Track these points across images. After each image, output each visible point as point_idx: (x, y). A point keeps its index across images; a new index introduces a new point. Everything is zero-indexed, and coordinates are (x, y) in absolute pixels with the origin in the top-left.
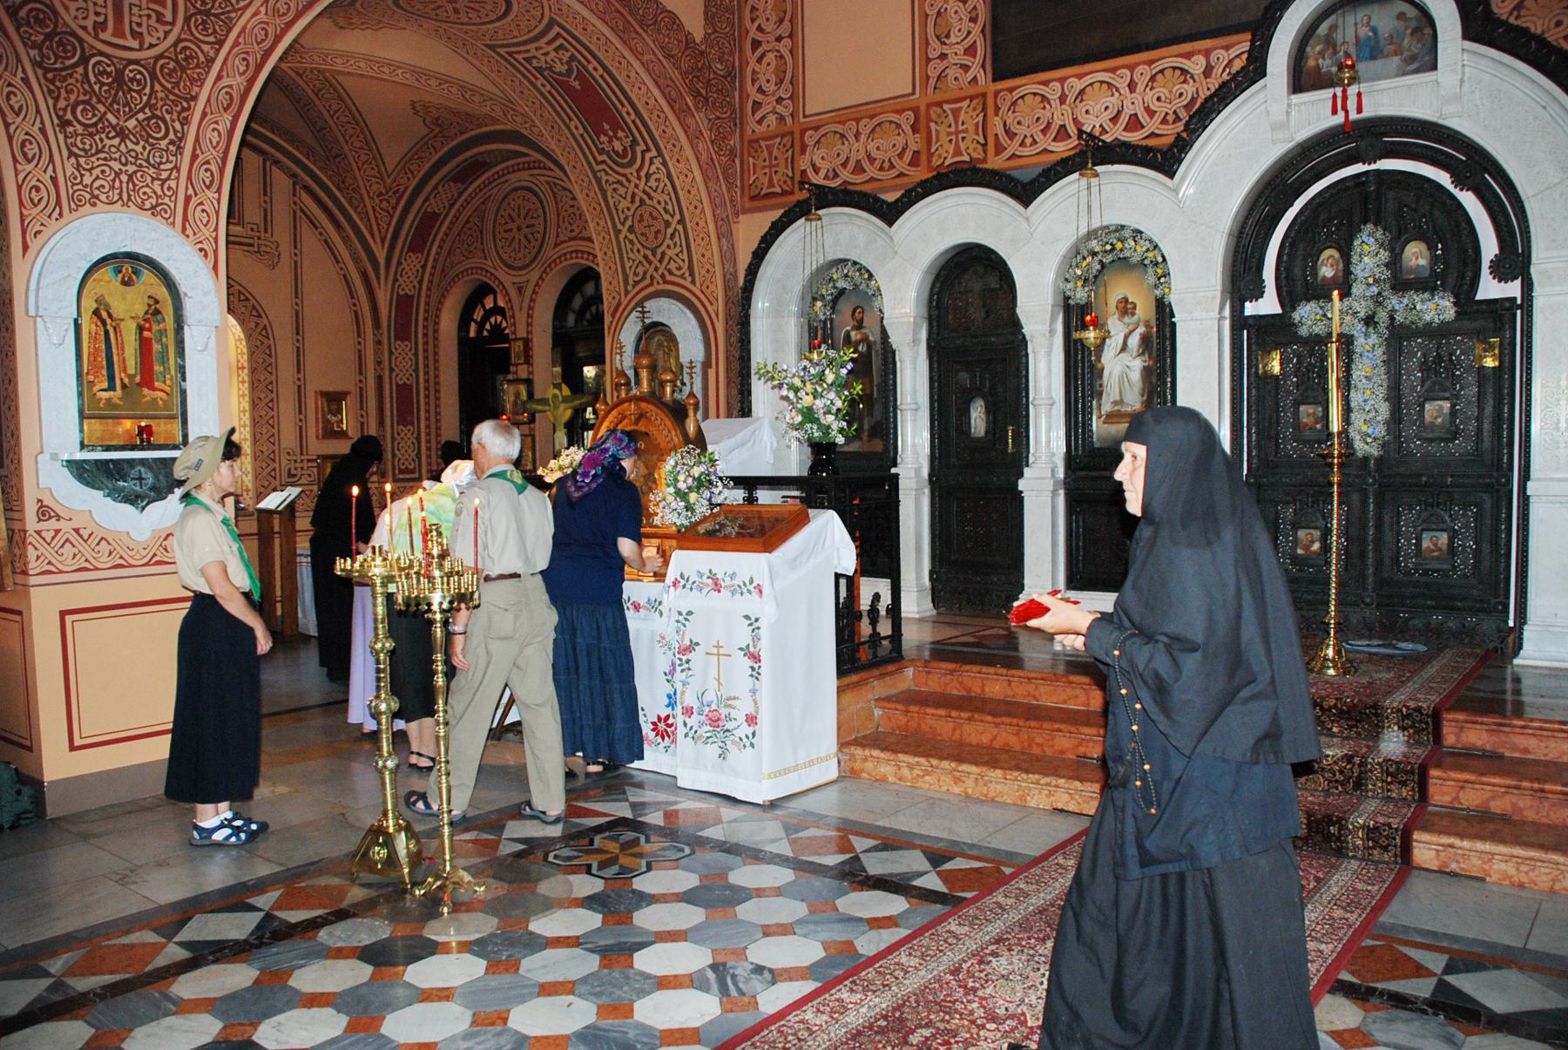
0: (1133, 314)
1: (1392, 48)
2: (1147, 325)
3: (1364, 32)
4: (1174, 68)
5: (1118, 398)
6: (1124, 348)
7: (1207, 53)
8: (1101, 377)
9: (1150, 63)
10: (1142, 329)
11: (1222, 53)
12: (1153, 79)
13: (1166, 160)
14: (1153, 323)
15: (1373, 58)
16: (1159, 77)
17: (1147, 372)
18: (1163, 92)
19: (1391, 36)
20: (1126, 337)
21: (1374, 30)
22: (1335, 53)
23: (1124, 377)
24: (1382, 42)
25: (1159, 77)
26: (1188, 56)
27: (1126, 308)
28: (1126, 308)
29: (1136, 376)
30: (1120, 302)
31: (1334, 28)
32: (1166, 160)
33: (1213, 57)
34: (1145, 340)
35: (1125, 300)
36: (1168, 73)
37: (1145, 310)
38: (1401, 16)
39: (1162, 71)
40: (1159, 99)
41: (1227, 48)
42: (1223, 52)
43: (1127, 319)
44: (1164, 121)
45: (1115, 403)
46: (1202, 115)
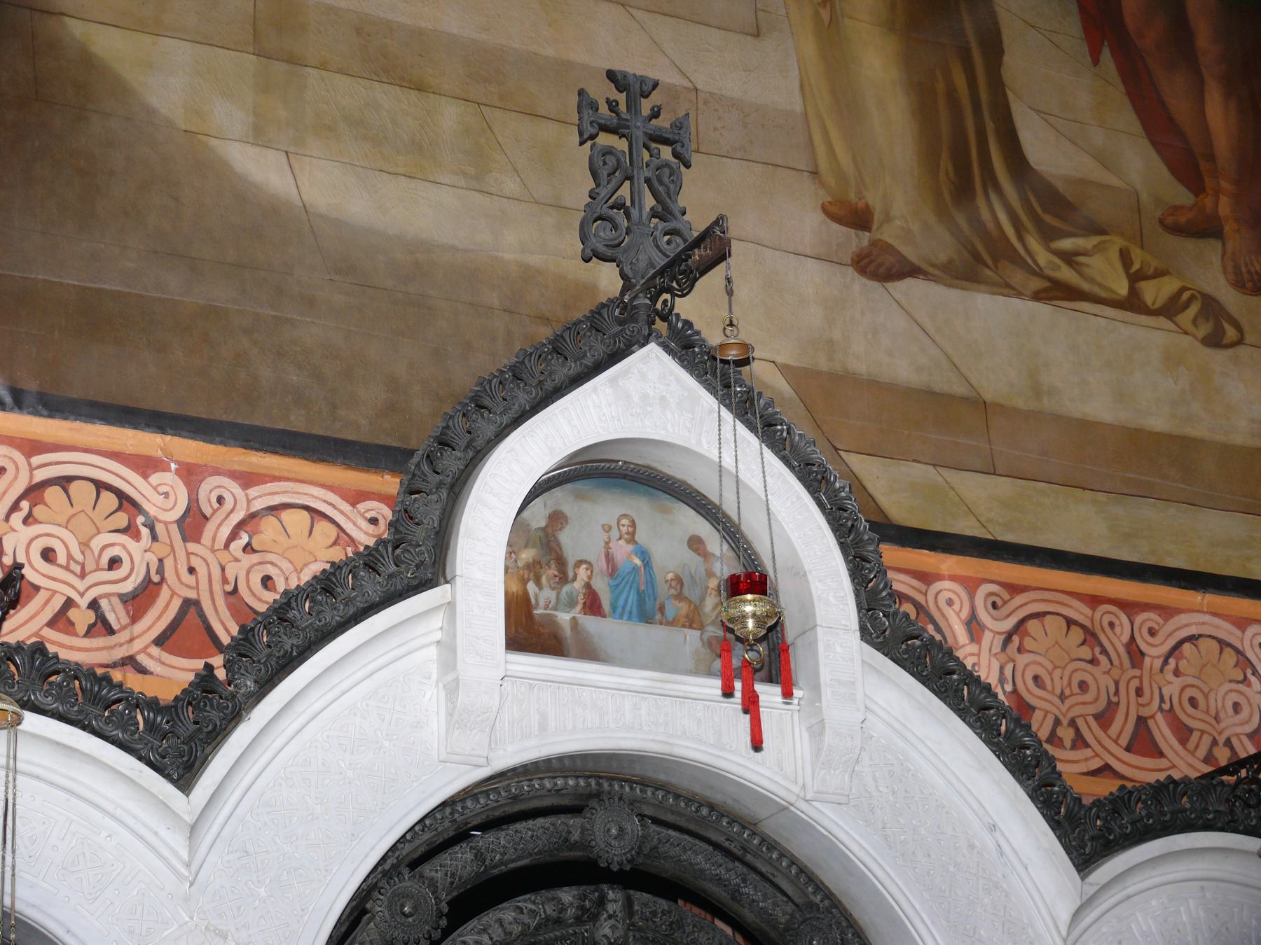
1: (683, 608)
3: (622, 550)
4: (100, 486)
7: (191, 474)
9: (32, 447)
11: (232, 489)
12: (34, 492)
13: (179, 738)
15: (645, 617)
16: (53, 493)
18: (65, 542)
19: (679, 580)
21: (644, 555)
22: (563, 578)
24: (663, 590)
25: (53, 493)
26: (145, 465)
32: (179, 738)
33: (209, 488)
36: (83, 491)
38: (696, 544)
39: (64, 482)
40: (48, 555)
41: (248, 480)
42: (235, 487)
44: (60, 620)
46: (281, 638)
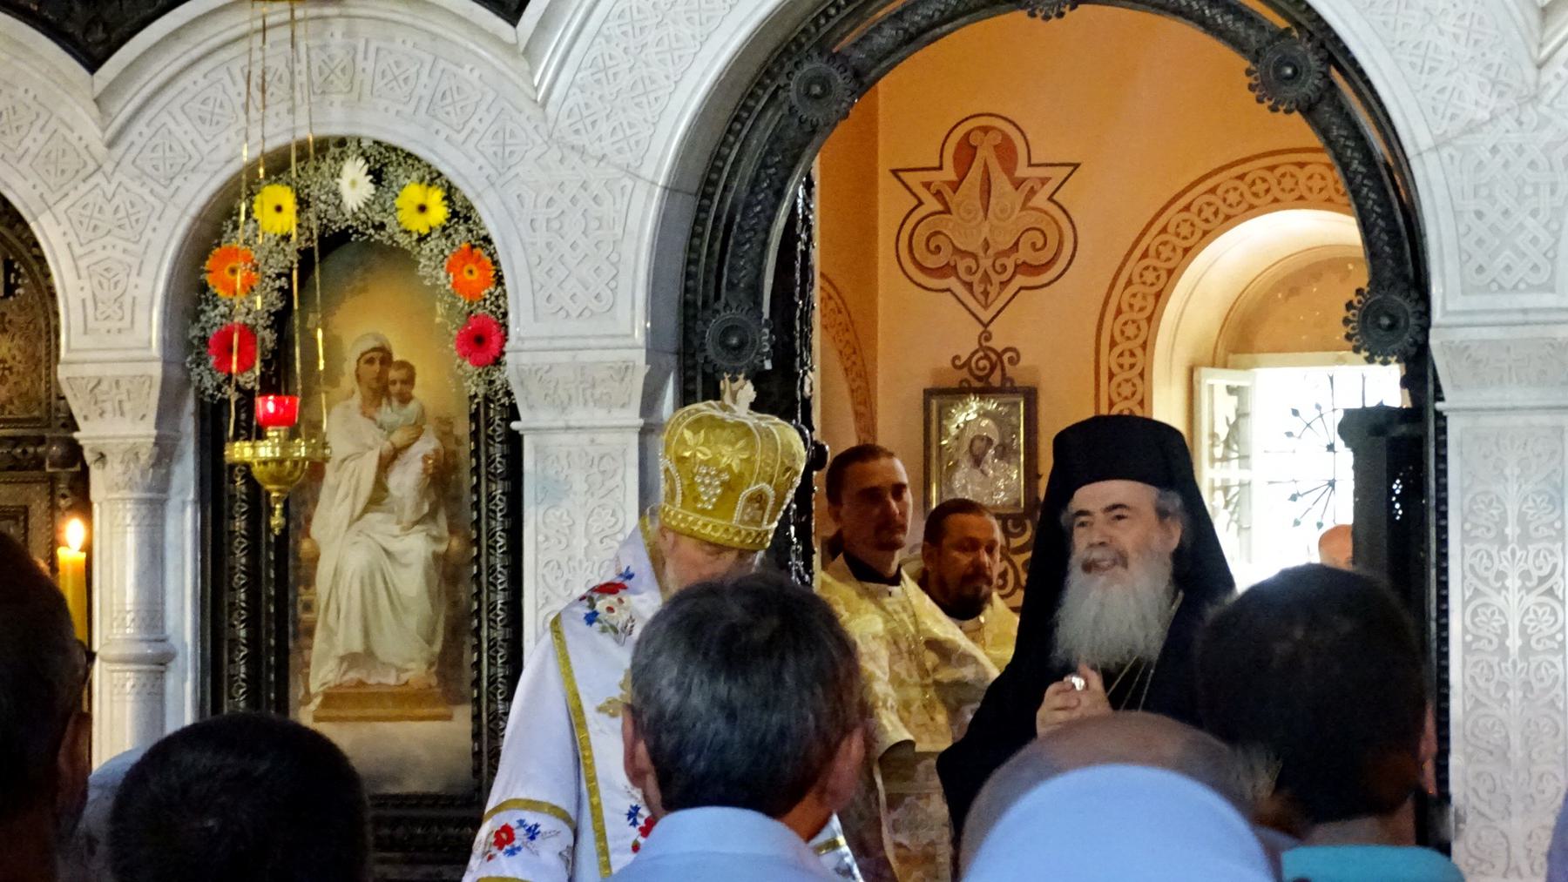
0: (405, 399)
2: (445, 434)
5: (357, 646)
6: (379, 497)
8: (309, 582)
10: (427, 445)
14: (463, 428)
17: (446, 572)
20: (386, 463)
23: (376, 581)
27: (385, 379)
28: (385, 379)
29: (412, 581)
30: (367, 359)
31: (483, 268)
34: (440, 479)
35: (383, 356)
37: (442, 380)
43: (388, 413)
45: (351, 660)
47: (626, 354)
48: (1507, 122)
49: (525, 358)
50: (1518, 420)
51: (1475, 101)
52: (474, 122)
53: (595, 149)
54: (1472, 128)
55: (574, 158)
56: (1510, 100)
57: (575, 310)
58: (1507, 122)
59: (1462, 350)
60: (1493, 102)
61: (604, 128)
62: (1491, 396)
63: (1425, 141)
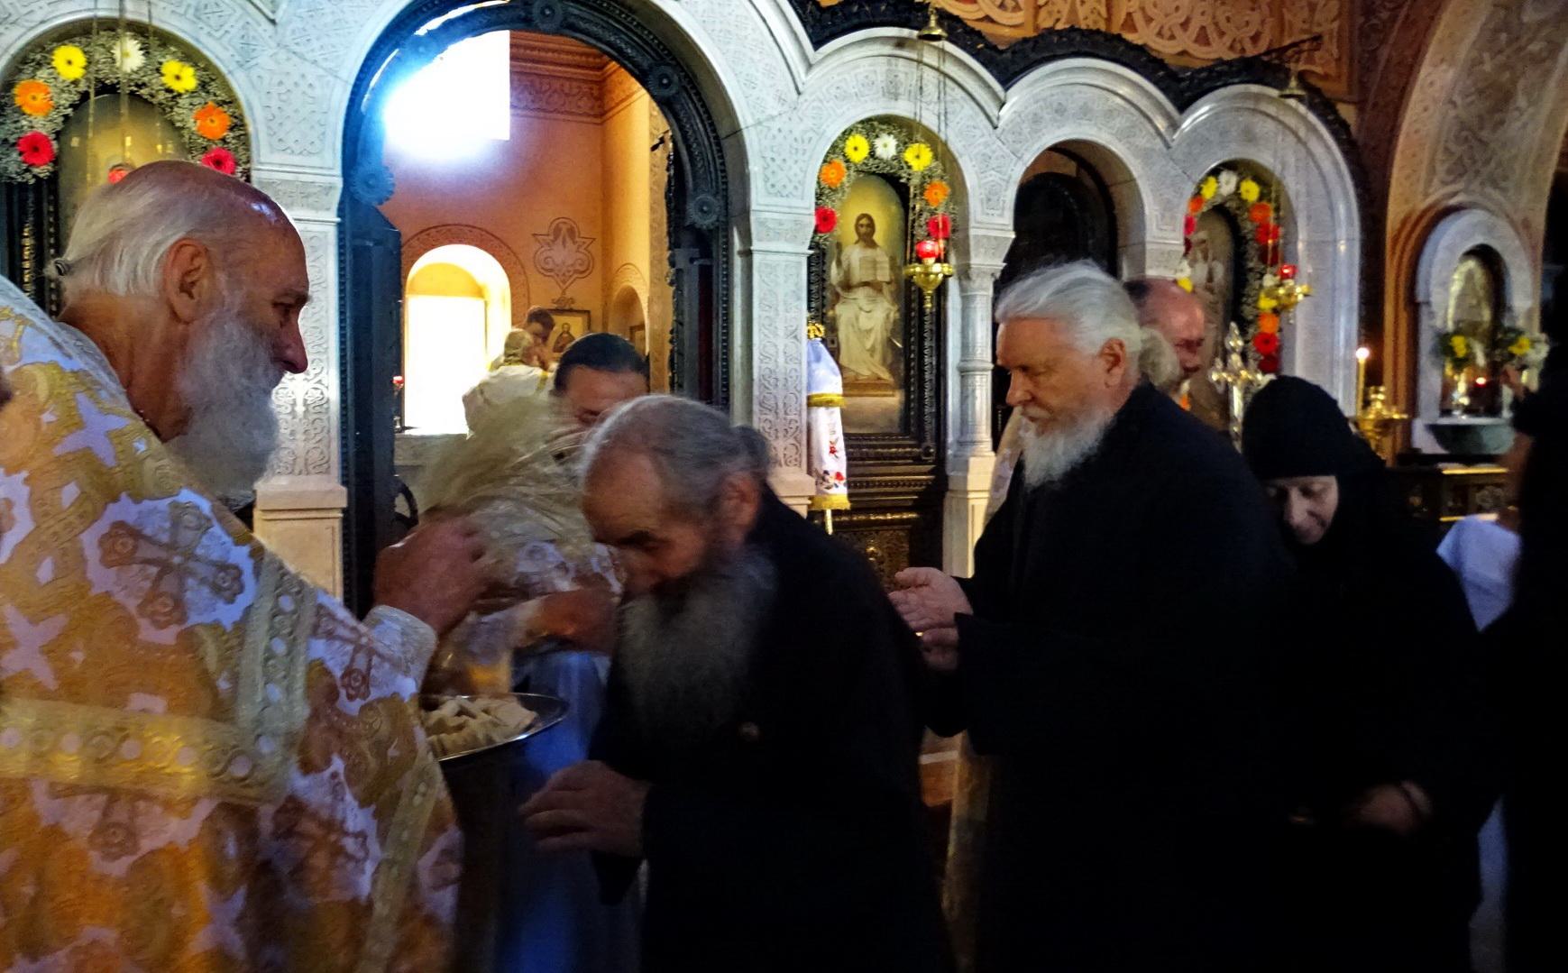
47: (329, 179)
48: (785, 117)
49: (264, 175)
50: (784, 257)
51: (773, 108)
52: (227, 27)
53: (310, 56)
54: (772, 118)
55: (295, 59)
56: (786, 108)
57: (297, 149)
58: (785, 117)
59: (762, 223)
60: (779, 108)
61: (315, 44)
62: (773, 246)
63: (750, 121)
